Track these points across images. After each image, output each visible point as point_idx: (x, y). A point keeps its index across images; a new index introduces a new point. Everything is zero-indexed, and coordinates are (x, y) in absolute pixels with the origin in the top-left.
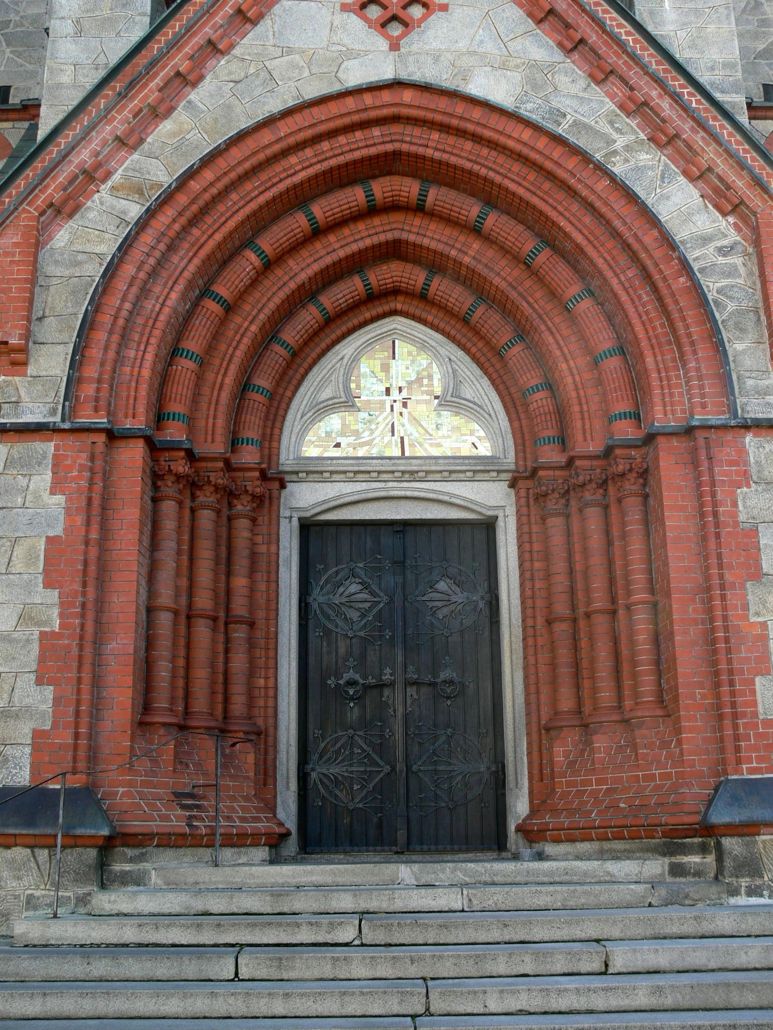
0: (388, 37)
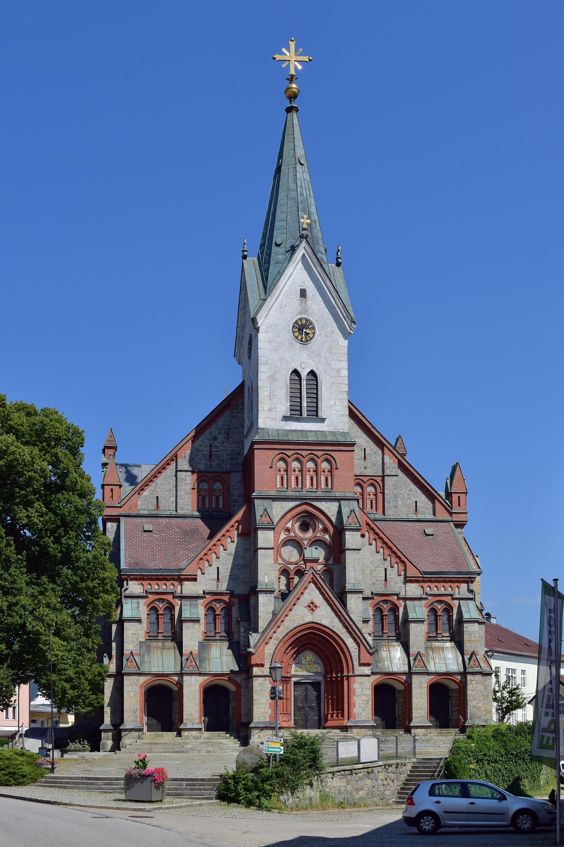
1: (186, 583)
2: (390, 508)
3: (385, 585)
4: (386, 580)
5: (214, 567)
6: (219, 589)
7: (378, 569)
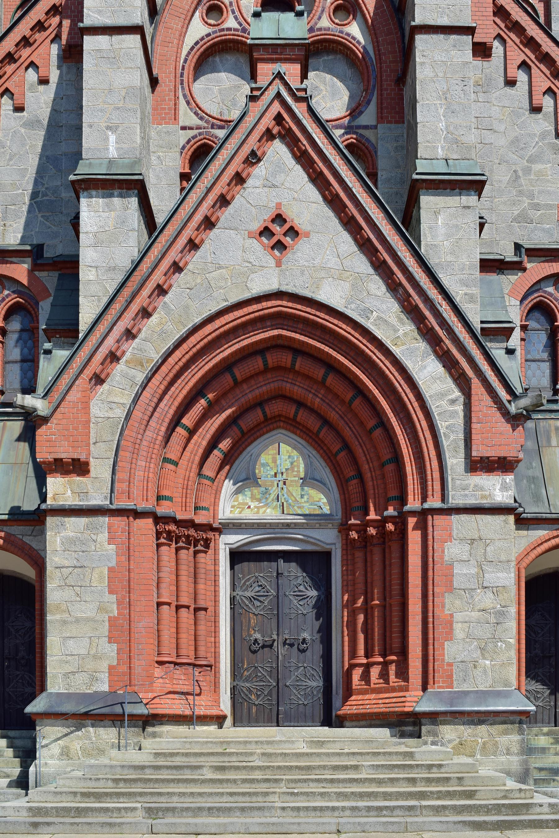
0: (274, 257)
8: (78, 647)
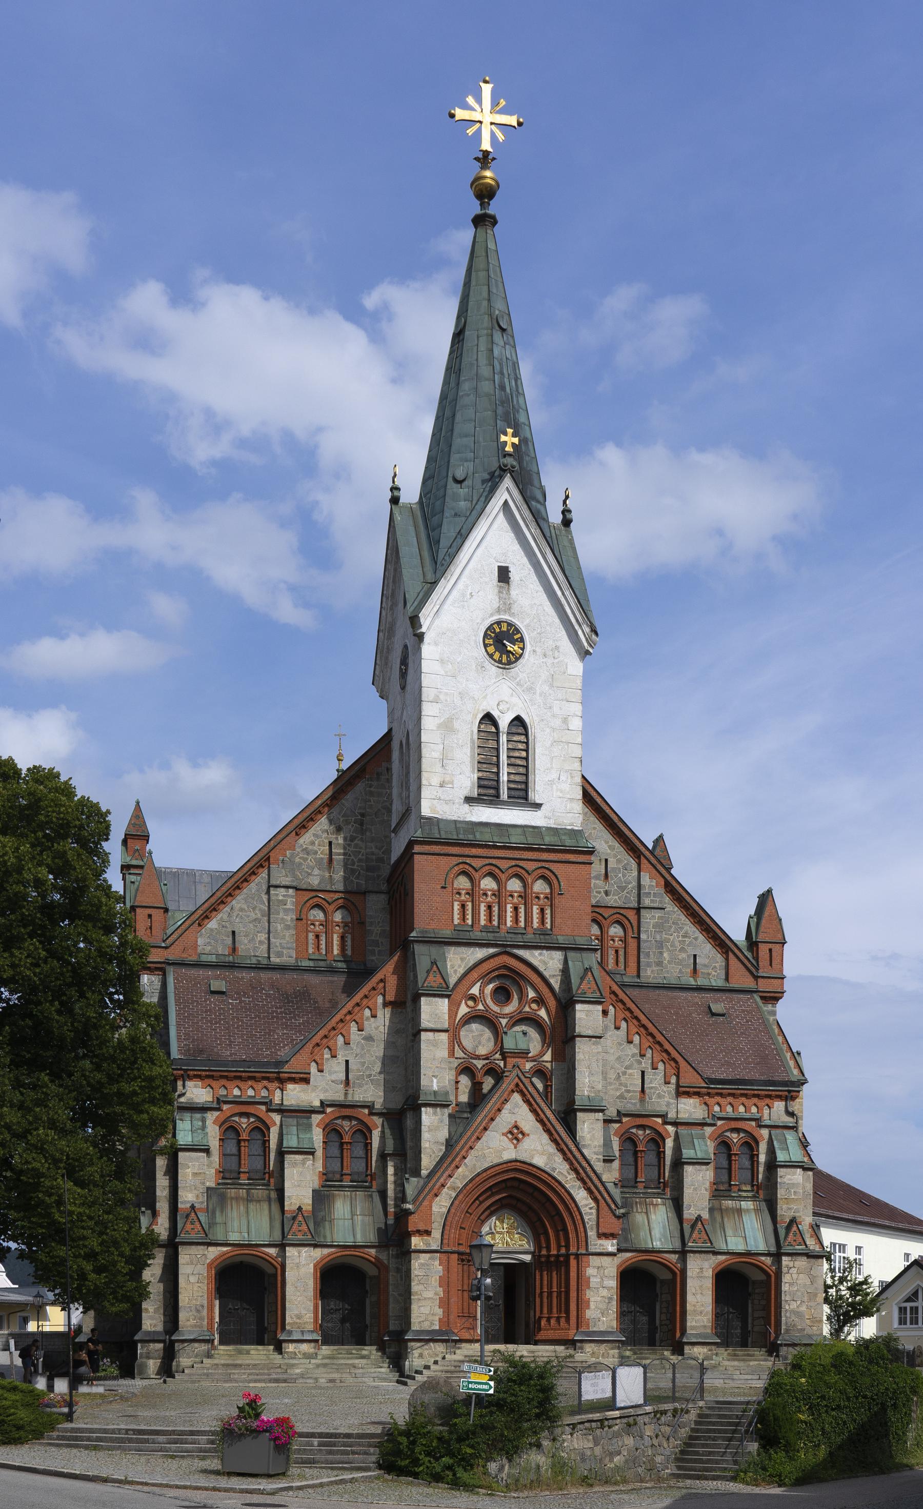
1: (290, 1086)
2: (649, 965)
3: (642, 1100)
4: (643, 1090)
5: (341, 1058)
6: (350, 1098)
7: (630, 1071)
8: (426, 1310)
